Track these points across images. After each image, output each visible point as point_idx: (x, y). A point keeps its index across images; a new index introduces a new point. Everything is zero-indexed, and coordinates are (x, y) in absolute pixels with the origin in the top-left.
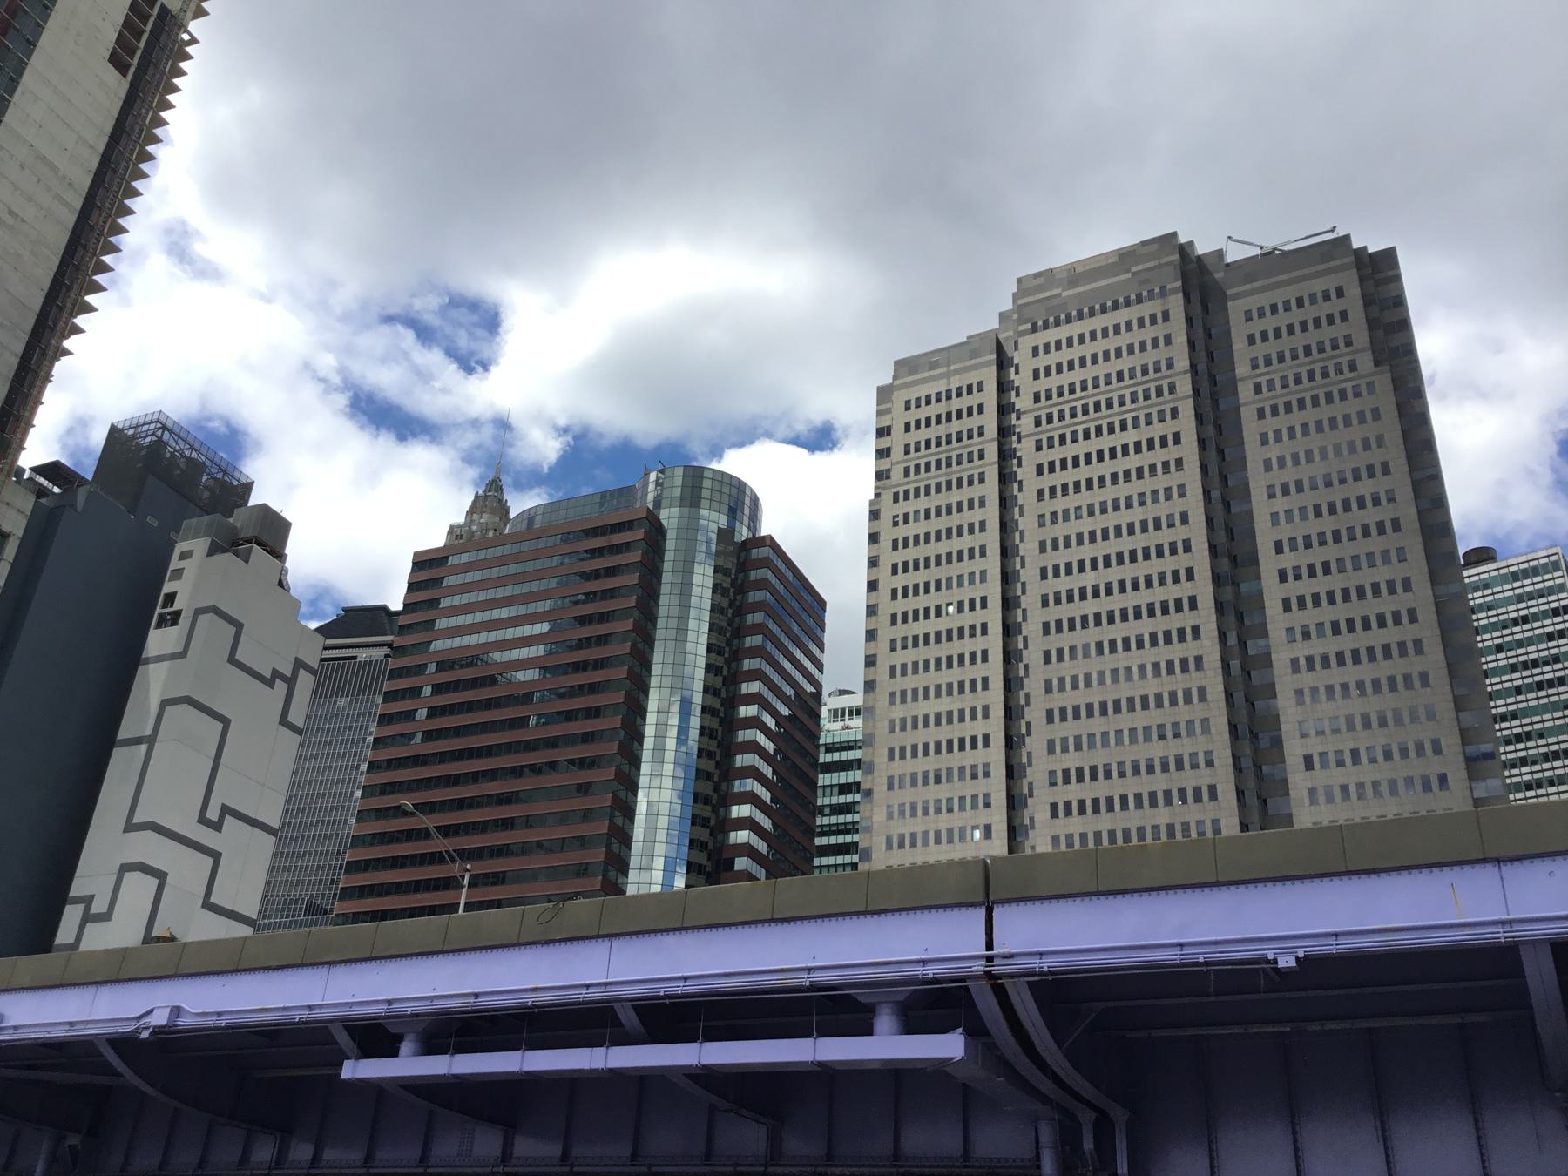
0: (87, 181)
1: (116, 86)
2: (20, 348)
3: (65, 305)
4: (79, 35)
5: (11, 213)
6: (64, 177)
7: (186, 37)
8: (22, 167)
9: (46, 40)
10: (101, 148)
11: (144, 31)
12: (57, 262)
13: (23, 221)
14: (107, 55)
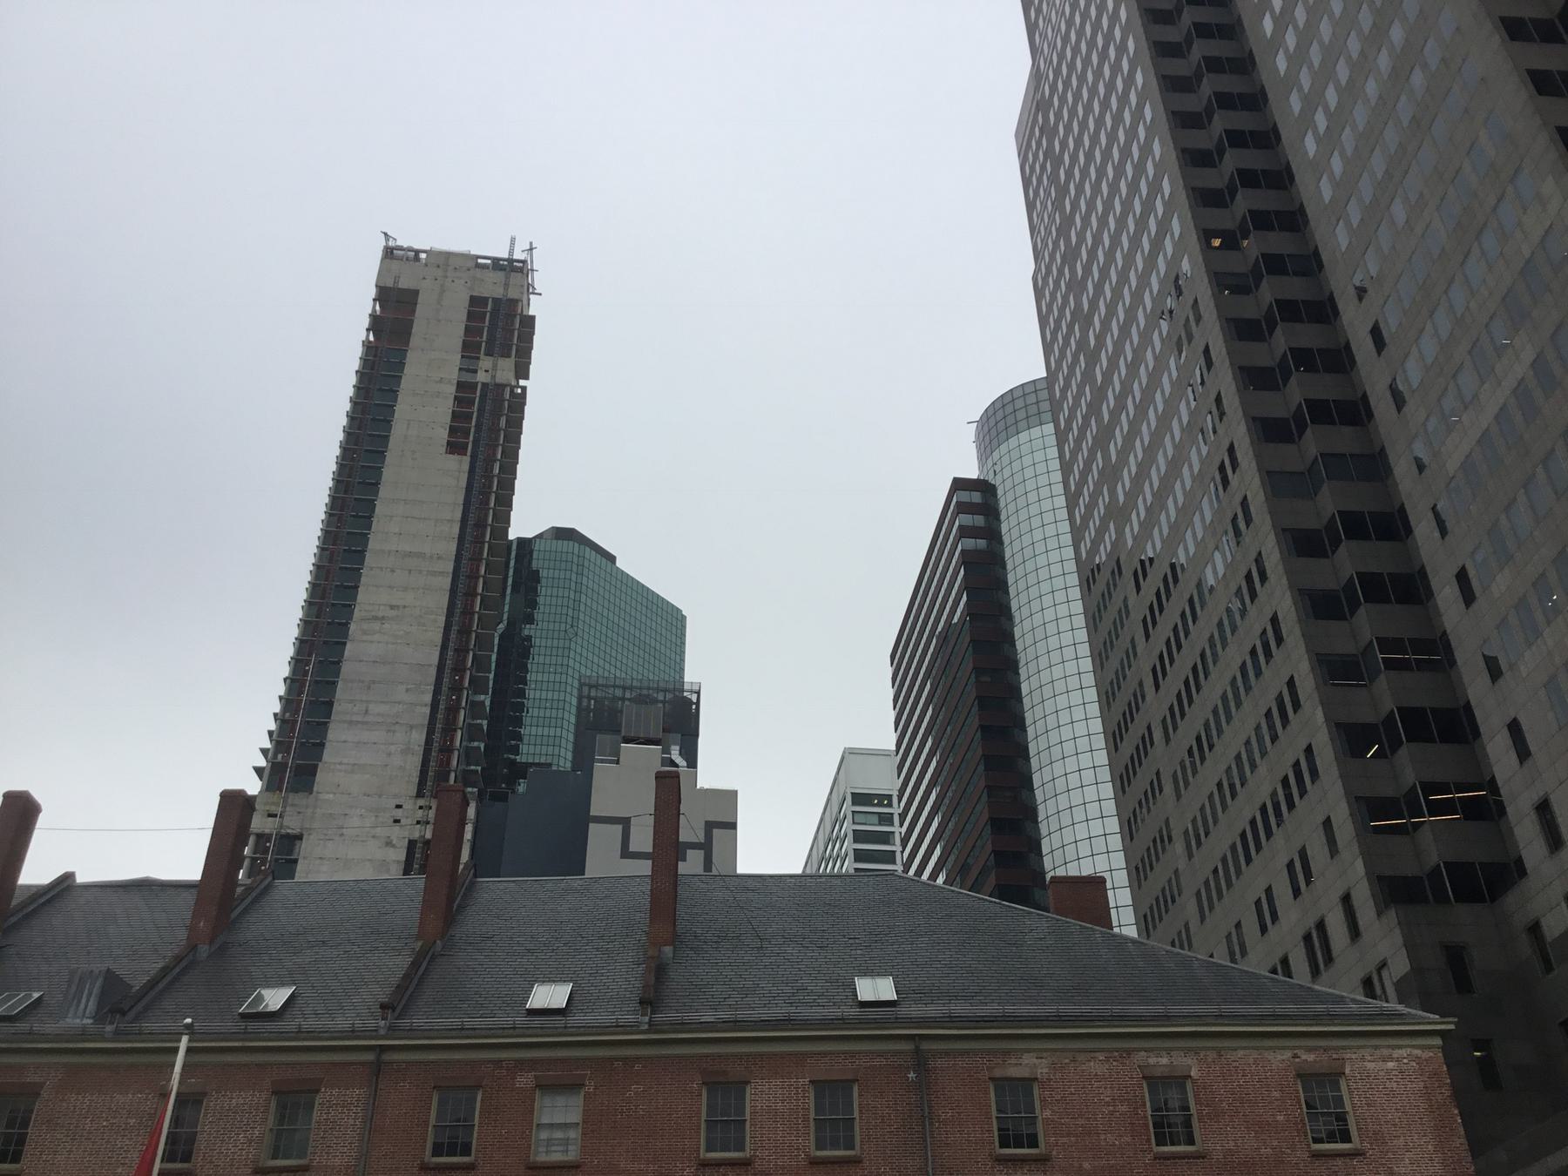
1: (459, 466)
5: (392, 607)
6: (431, 557)
8: (393, 571)
10: (458, 515)
13: (405, 607)
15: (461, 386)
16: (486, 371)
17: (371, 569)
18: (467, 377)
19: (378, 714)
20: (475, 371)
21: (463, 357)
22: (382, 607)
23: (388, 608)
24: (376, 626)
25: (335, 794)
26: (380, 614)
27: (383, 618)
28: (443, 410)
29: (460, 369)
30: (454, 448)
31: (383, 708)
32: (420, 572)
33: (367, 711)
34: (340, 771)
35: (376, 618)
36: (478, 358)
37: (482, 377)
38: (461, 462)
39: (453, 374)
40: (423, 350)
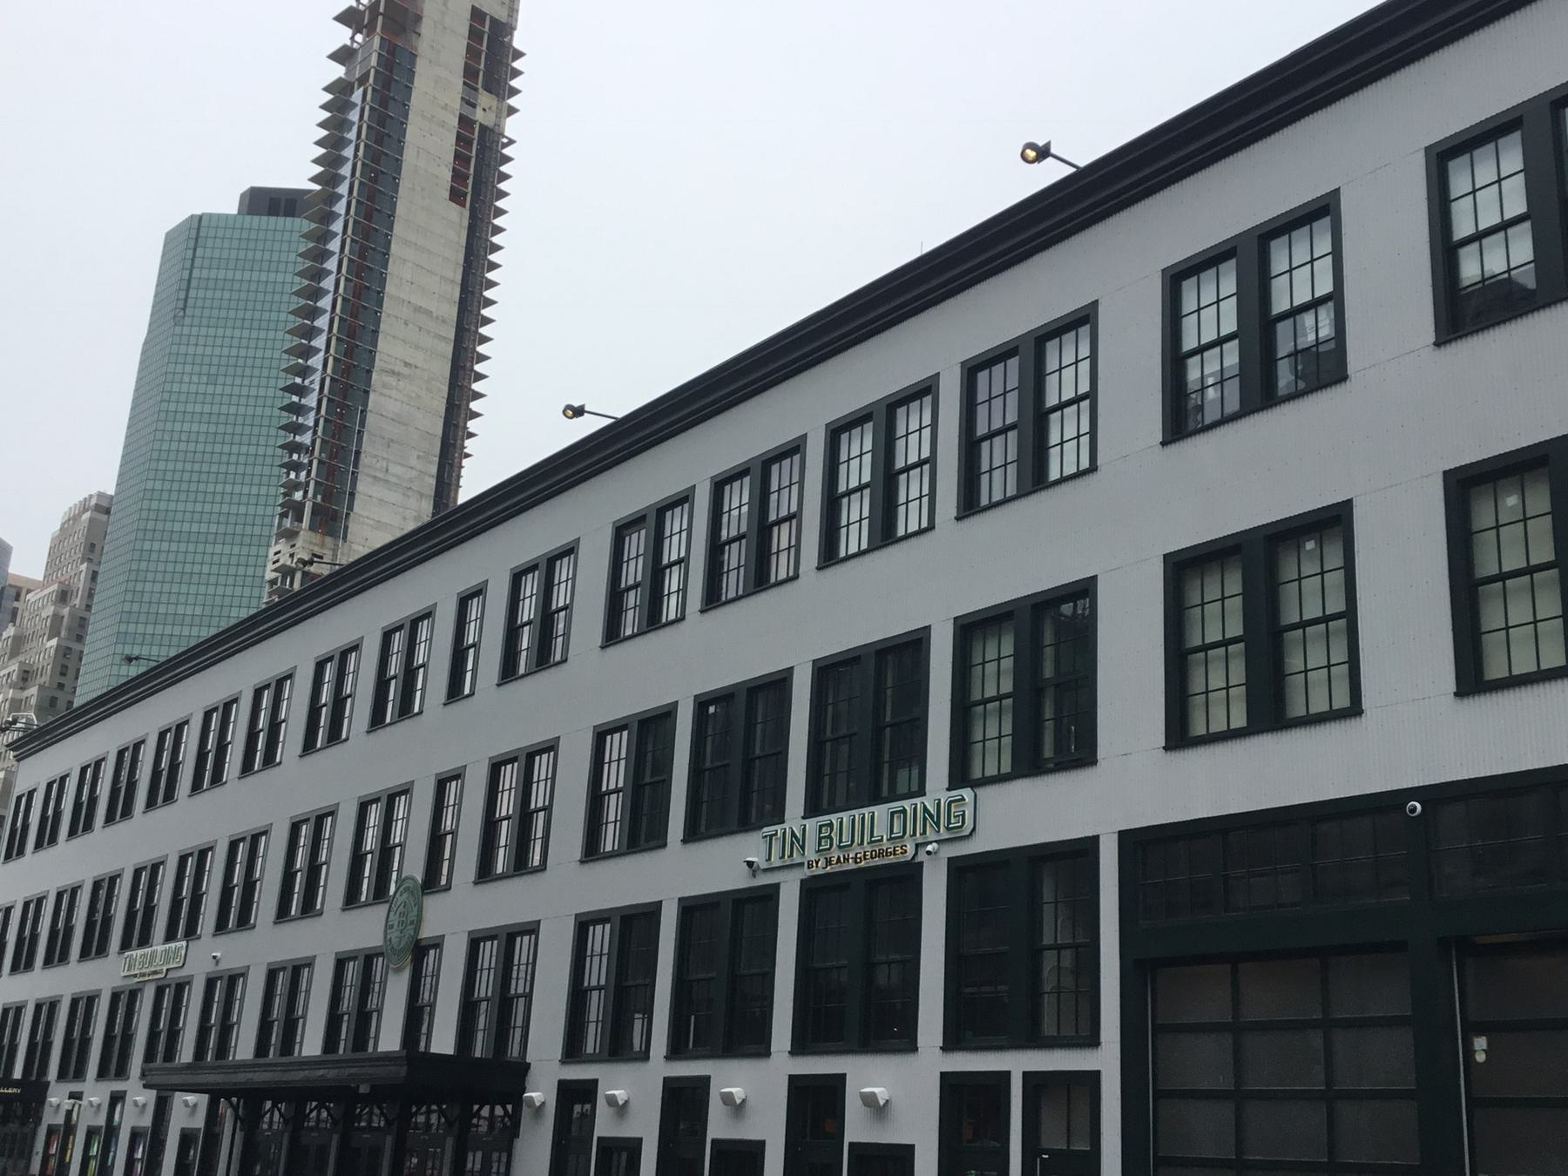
0: (453, 312)
1: (458, 217)
2: (434, 470)
3: (458, 422)
4: (423, 189)
5: (407, 364)
6: (437, 318)
7: (505, 140)
8: (406, 324)
9: (401, 209)
10: (459, 278)
11: (471, 157)
12: (446, 389)
13: (416, 367)
14: (447, 195)
15: (465, 122)
16: (484, 110)
17: (389, 315)
18: (467, 111)
19: (394, 475)
20: (474, 106)
21: (465, 83)
22: (398, 362)
23: (402, 364)
24: (392, 380)
25: (364, 546)
26: (396, 370)
27: (399, 374)
28: (446, 145)
29: (462, 98)
30: (456, 196)
31: (395, 469)
32: (429, 332)
33: (387, 470)
34: (367, 524)
35: (393, 373)
36: (476, 90)
37: (479, 116)
38: (461, 213)
39: (456, 105)
40: (430, 62)
